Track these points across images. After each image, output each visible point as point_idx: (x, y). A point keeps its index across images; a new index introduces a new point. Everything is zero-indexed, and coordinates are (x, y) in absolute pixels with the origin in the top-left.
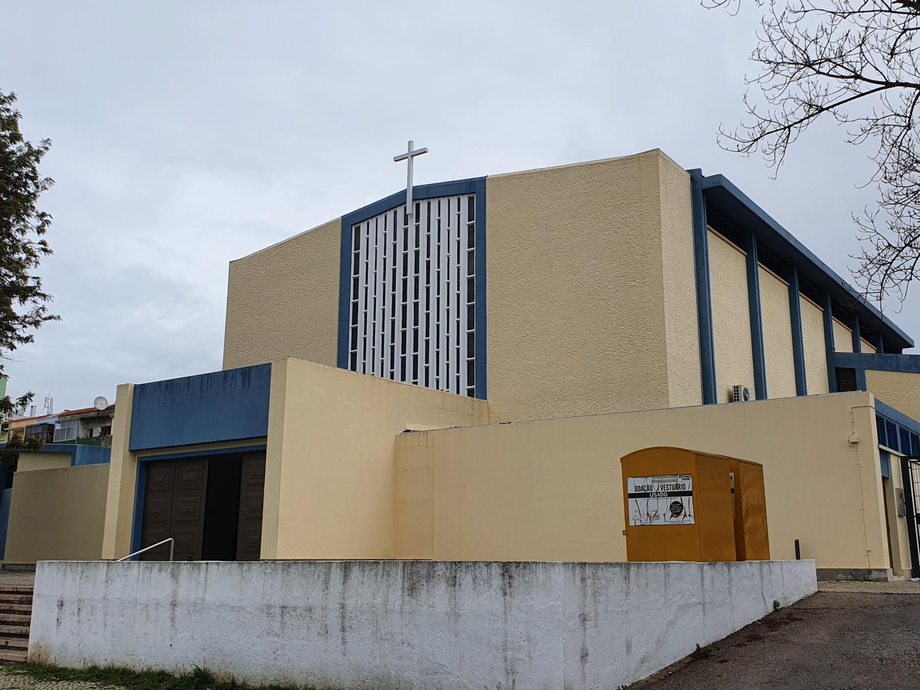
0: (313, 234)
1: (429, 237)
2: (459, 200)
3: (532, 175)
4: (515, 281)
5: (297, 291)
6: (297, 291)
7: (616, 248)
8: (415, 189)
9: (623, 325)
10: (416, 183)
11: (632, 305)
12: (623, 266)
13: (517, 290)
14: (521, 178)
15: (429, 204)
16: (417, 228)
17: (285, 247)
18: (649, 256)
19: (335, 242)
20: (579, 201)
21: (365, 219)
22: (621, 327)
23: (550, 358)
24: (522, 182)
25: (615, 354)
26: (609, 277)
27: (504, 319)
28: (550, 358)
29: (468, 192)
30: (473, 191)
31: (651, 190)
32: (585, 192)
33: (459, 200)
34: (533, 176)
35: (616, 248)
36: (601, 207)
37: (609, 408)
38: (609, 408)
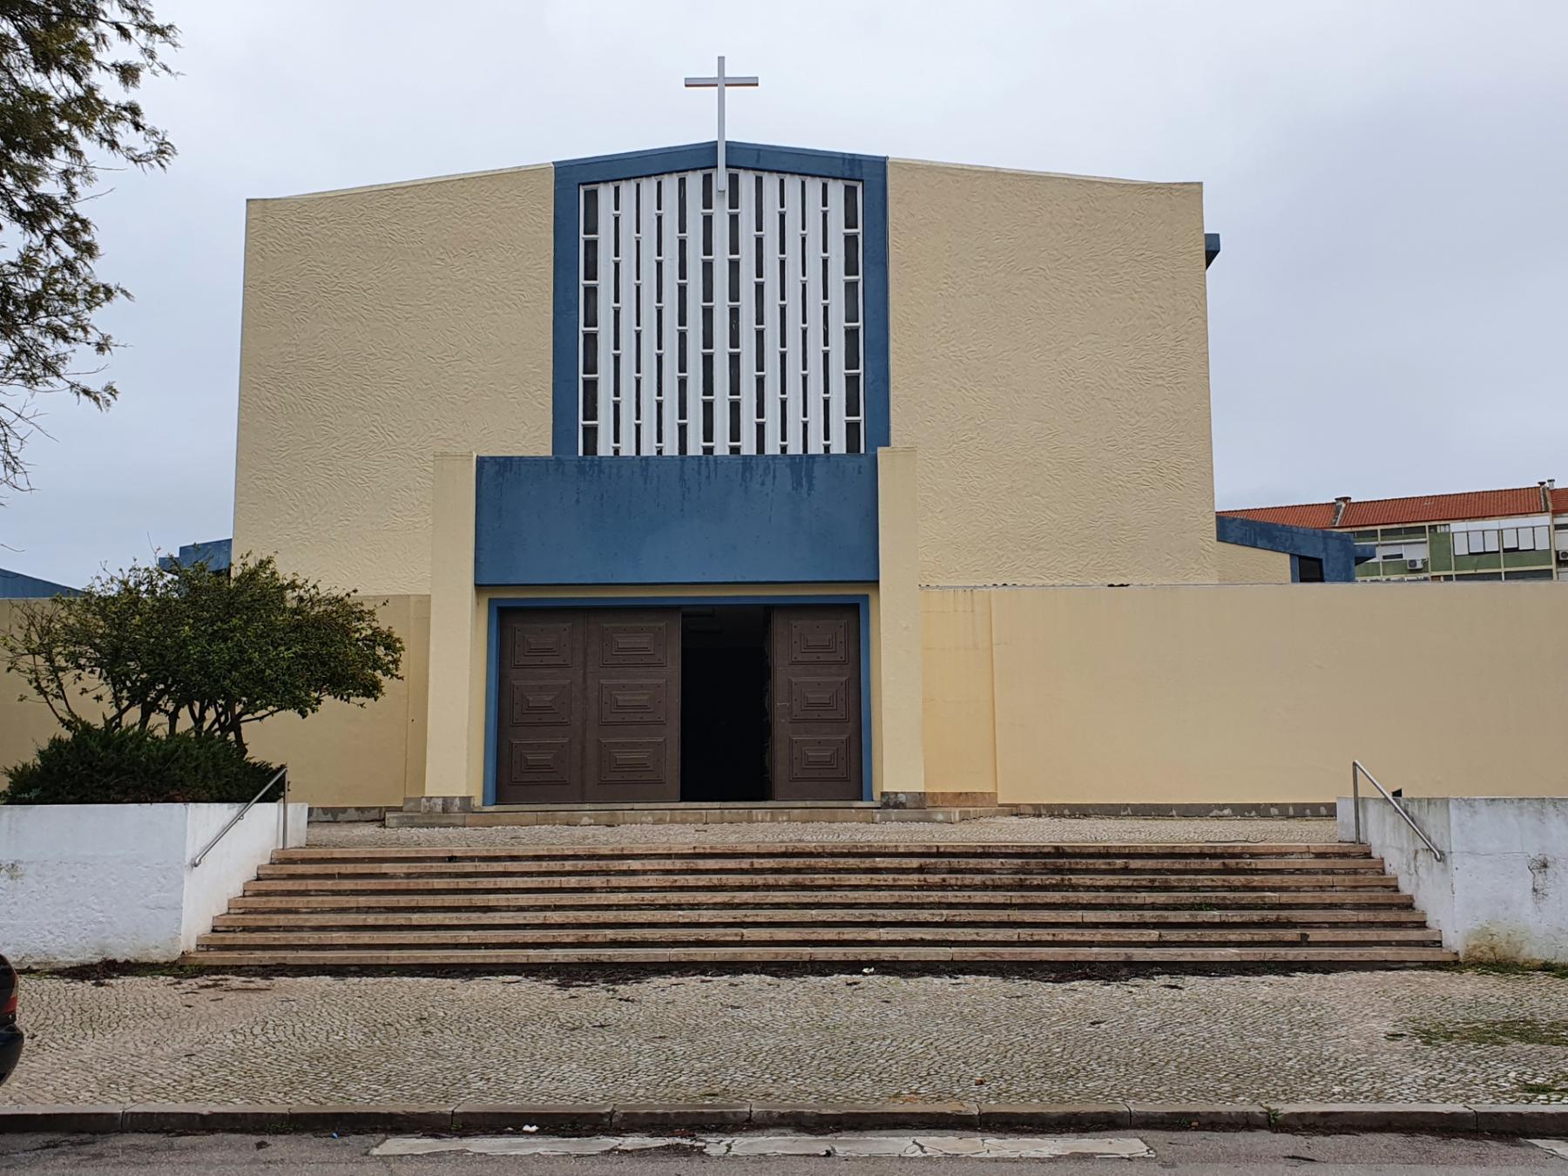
0: (483, 183)
1: (759, 241)
2: (617, 189)
3: (978, 175)
4: (947, 348)
5: (441, 288)
6: (441, 288)
7: (1131, 323)
8: (731, 147)
9: (1143, 443)
10: (731, 136)
11: (1157, 414)
12: (1143, 353)
13: (950, 362)
14: (957, 176)
15: (682, 182)
16: (734, 219)
17: (406, 196)
18: (1187, 344)
19: (539, 209)
20: (1066, 235)
21: (776, 168)
22: (1141, 447)
23: (1014, 481)
24: (958, 182)
25: (1129, 485)
26: (1121, 366)
27: (925, 407)
28: (1014, 481)
29: (846, 175)
30: (857, 176)
31: (1191, 244)
32: (1076, 224)
33: (617, 189)
34: (979, 177)
35: (1131, 323)
36: (1105, 254)
37: (1118, 567)
38: (1118, 567)
